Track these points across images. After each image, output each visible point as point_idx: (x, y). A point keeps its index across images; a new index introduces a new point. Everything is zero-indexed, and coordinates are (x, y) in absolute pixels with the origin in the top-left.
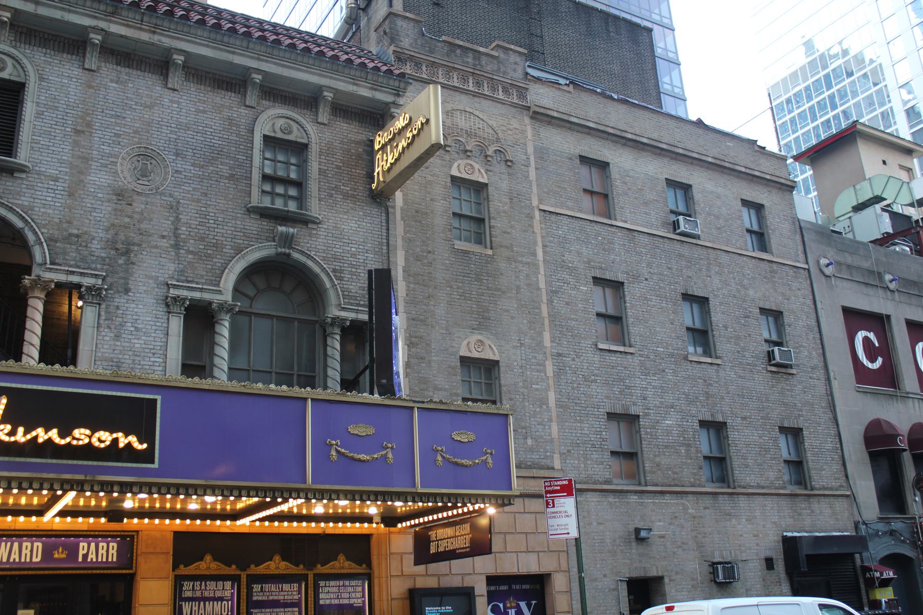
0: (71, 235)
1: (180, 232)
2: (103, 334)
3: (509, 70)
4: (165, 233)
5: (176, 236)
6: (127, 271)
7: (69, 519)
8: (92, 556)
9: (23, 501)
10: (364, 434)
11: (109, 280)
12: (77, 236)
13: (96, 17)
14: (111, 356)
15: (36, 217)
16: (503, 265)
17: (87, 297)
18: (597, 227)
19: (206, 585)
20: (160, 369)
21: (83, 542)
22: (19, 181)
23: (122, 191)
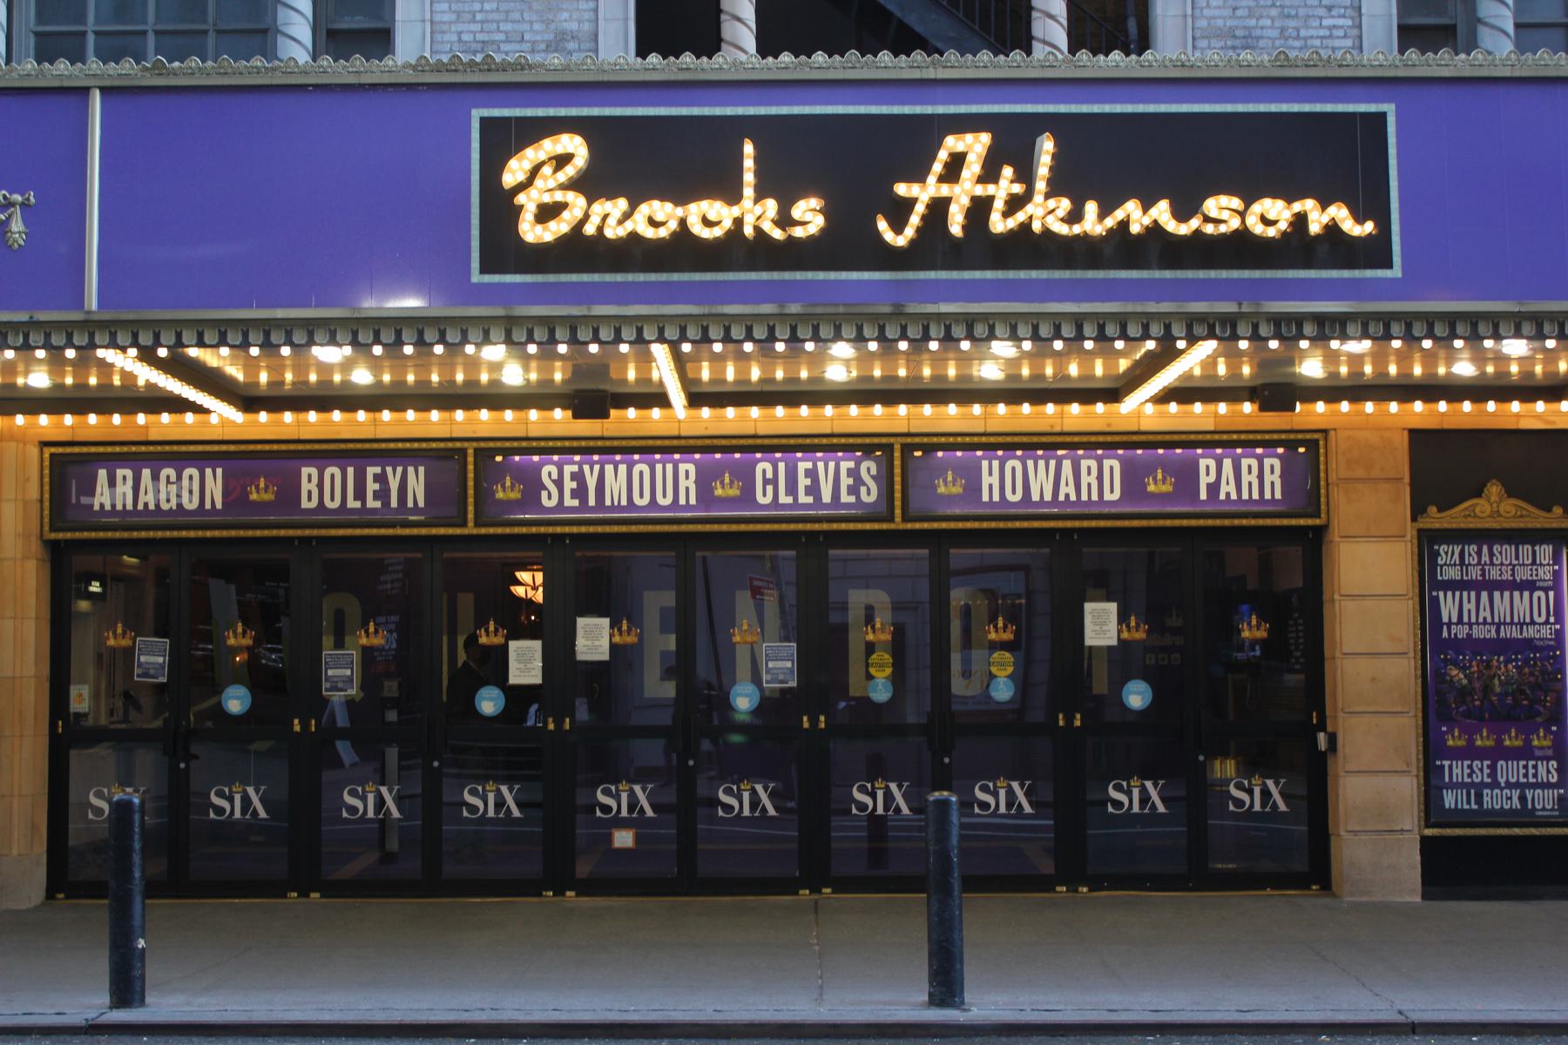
7: (1173, 407)
8: (1227, 489)
9: (1073, 370)
14: (1230, 23)
19: (1491, 555)
20: (1349, 43)
21: (1203, 456)
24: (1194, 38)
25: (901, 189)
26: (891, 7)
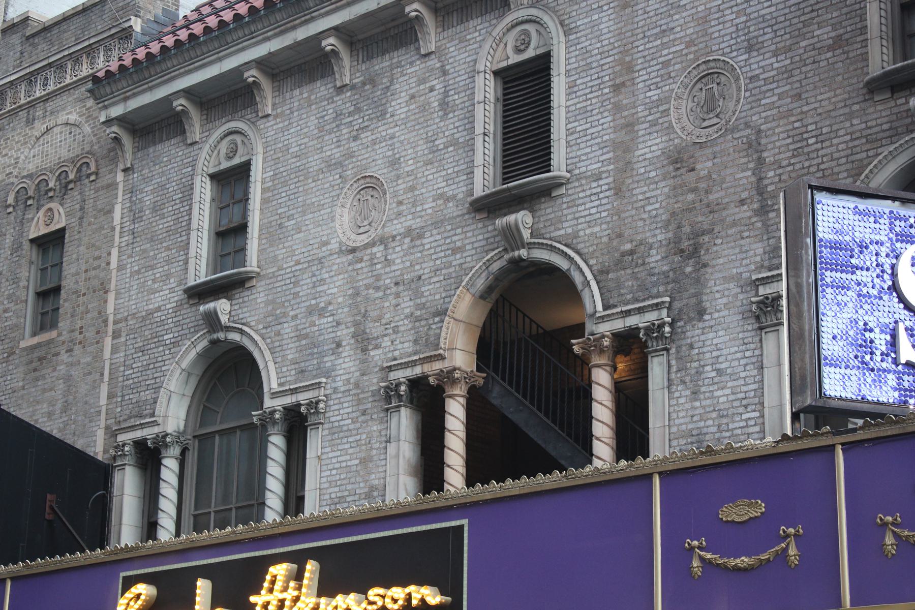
0: (623, 254)
1: (766, 182)
2: (677, 394)
4: (744, 195)
5: (761, 191)
6: (698, 281)
10: (747, 517)
11: (677, 305)
12: (632, 252)
14: (690, 426)
15: (582, 245)
17: (650, 345)
20: (757, 429)
22: (559, 201)
23: (679, 153)
24: (670, 440)
25: (253, 599)
26: (540, 442)
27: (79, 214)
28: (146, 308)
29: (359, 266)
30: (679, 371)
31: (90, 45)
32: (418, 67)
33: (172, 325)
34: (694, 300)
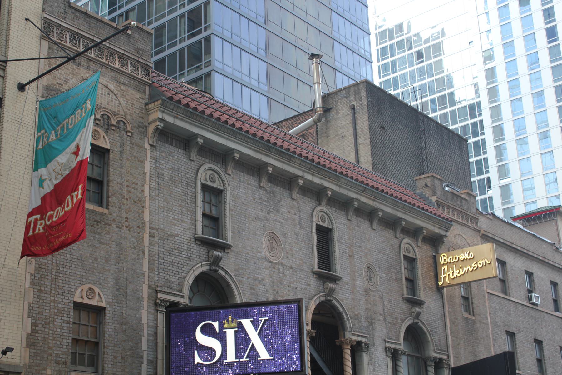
0: (355, 315)
3: (472, 208)
4: (381, 313)
12: (357, 316)
13: (357, 193)
16: (478, 325)
18: (505, 301)
26: (322, 367)
27: (120, 149)
28: (170, 230)
29: (274, 270)
30: (370, 360)
31: (124, 54)
32: (289, 200)
33: (186, 248)
34: (372, 339)
